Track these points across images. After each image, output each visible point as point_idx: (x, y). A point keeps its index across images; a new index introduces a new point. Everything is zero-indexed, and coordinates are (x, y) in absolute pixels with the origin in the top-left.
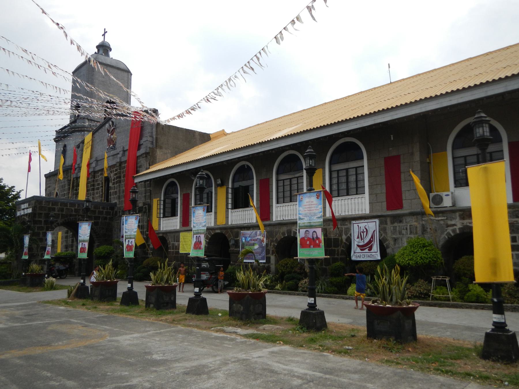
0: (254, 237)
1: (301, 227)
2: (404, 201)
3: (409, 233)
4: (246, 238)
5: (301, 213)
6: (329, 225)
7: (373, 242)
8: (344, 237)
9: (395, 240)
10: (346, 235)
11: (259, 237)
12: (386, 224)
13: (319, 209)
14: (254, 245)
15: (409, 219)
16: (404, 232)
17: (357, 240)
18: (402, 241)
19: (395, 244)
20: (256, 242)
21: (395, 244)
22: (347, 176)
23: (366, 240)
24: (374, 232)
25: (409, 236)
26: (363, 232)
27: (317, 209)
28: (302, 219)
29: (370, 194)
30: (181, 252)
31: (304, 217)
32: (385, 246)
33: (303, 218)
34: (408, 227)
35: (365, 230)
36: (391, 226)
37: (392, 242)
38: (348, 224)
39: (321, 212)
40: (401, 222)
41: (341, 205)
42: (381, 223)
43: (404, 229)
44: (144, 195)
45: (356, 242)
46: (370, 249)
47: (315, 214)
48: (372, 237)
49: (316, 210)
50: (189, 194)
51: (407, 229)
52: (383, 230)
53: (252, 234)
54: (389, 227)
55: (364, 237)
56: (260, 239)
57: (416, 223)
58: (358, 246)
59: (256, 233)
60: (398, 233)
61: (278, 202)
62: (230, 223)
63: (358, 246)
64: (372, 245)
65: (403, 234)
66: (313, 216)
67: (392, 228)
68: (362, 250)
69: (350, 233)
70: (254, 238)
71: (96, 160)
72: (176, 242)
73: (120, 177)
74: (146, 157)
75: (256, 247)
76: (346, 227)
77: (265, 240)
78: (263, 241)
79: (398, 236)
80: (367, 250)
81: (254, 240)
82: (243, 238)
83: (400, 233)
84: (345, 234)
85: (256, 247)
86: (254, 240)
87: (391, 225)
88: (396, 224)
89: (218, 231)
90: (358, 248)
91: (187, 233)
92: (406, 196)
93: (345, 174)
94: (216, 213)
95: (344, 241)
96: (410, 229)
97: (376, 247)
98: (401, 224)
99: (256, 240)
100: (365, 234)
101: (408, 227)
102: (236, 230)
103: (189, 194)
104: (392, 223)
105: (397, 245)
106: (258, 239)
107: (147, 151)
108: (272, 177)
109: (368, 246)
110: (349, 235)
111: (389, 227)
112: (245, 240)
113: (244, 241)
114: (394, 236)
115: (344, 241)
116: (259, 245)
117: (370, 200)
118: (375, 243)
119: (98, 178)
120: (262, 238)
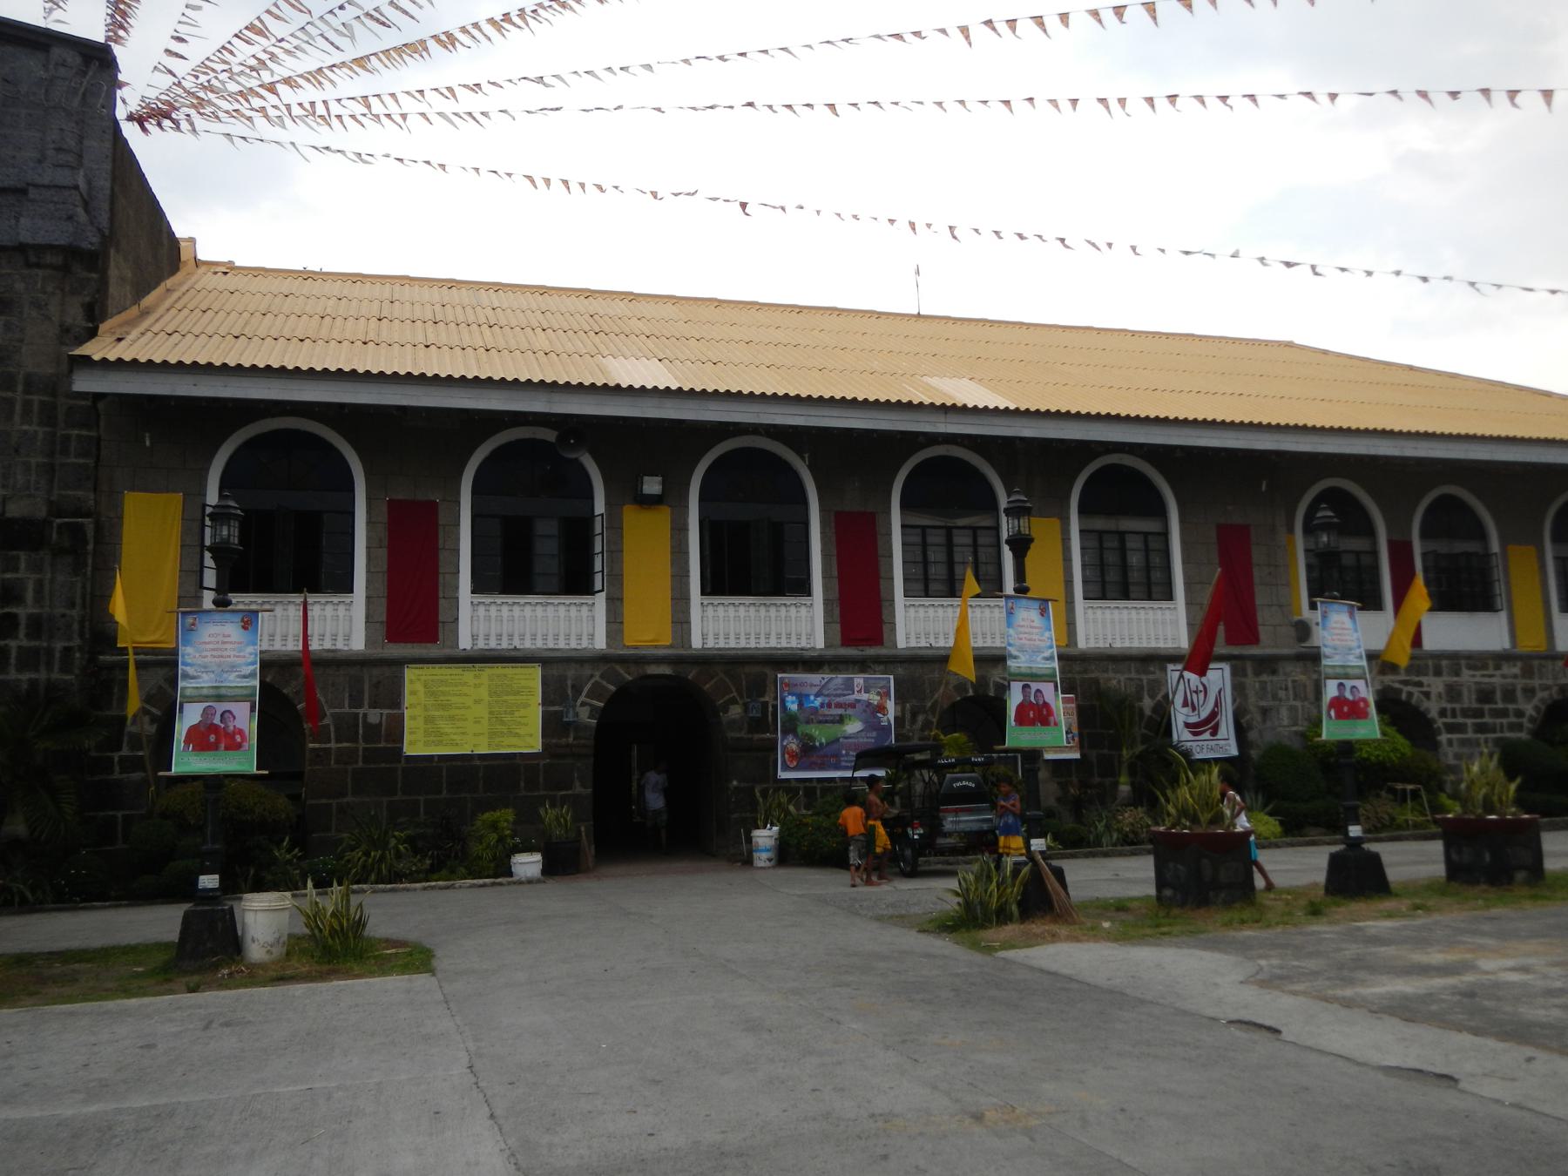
0: (839, 696)
1: (1020, 676)
2: (1261, 629)
3: (1291, 697)
4: (801, 698)
5: (189, 661)
6: (1104, 671)
7: (1219, 717)
8: (1147, 704)
9: (1265, 712)
10: (1152, 697)
11: (864, 697)
12: (1245, 675)
13: (247, 655)
14: (841, 720)
15: (1289, 667)
16: (1282, 694)
17: (1186, 710)
18: (1278, 713)
19: (1264, 721)
20: (850, 711)
21: (1264, 721)
22: (1123, 551)
23: (1205, 714)
24: (1220, 692)
25: (1293, 703)
26: (1196, 692)
27: (242, 654)
28: (193, 678)
29: (1189, 603)
30: (410, 749)
31: (199, 674)
32: (1245, 725)
33: (195, 674)
34: (1290, 685)
35: (1201, 688)
36: (1255, 682)
37: (1258, 718)
38: (1158, 672)
39: (253, 663)
40: (1274, 672)
41: (1113, 621)
42: (1234, 674)
43: (1281, 689)
44: (41, 459)
45: (1180, 716)
46: (1215, 731)
47: (233, 667)
48: (1216, 705)
49: (238, 657)
50: (432, 508)
51: (1286, 689)
52: (1238, 689)
53: (832, 685)
54: (1251, 681)
55: (1201, 702)
56: (869, 704)
57: (1303, 677)
58: (1187, 725)
59: (849, 686)
60: (1270, 696)
62: (696, 643)
63: (1187, 725)
64: (1218, 721)
65: (1280, 700)
66: (227, 672)
67: (1257, 685)
68: (1195, 734)
69: (1162, 693)
70: (841, 700)
72: (374, 705)
74: (65, 269)
75: (853, 727)
76: (1151, 677)
77: (891, 706)
78: (881, 708)
79: (1271, 703)
80: (1207, 736)
81: (839, 706)
83: (1275, 697)
84: (1149, 695)
85: (853, 727)
86: (839, 706)
87: (1256, 680)
88: (1265, 677)
89: (665, 670)
90: (1186, 730)
91: (459, 671)
92: (1266, 618)
93: (1115, 544)
94: (615, 604)
95: (1148, 712)
96: (1294, 688)
97: (1227, 728)
98: (1275, 678)
99: (852, 705)
100: (1201, 696)
101: (1290, 685)
102: (756, 669)
104: (1257, 673)
105: (1269, 724)
106: (858, 701)
107: (85, 245)
109: (1209, 724)
110: (1159, 697)
111: (1251, 681)
112: (800, 705)
114: (1263, 703)
115: (1148, 712)
116: (865, 722)
117: (1188, 618)
118: (1224, 718)
120: (875, 699)
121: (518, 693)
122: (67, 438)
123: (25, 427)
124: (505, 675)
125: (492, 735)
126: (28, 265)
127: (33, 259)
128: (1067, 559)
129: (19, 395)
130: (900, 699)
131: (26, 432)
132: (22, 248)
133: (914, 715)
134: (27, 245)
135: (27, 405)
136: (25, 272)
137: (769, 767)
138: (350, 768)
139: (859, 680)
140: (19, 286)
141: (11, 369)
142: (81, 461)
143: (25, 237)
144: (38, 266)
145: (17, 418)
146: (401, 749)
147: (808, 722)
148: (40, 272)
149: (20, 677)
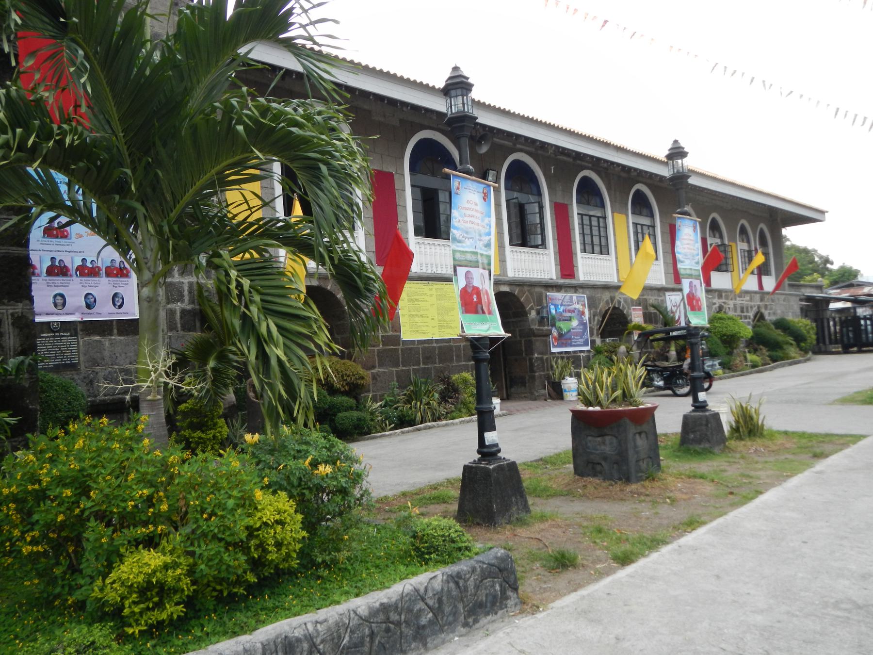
0: (569, 305)
4: (556, 306)
20: (573, 315)
30: (405, 337)
53: (565, 300)
56: (579, 311)
61: (584, 250)
70: (569, 308)
75: (575, 323)
78: (583, 313)
81: (569, 311)
82: (552, 307)
85: (575, 323)
86: (569, 311)
91: (422, 286)
99: (573, 311)
102: (538, 290)
103: (391, 175)
106: (575, 309)
108: (572, 204)
112: (556, 310)
113: (553, 311)
116: (579, 321)
121: (449, 301)
124: (443, 289)
125: (441, 327)
128: (629, 237)
130: (590, 308)
133: (594, 316)
137: (547, 346)
138: (376, 349)
139: (575, 296)
146: (400, 336)
147: (560, 320)
149: (182, 280)
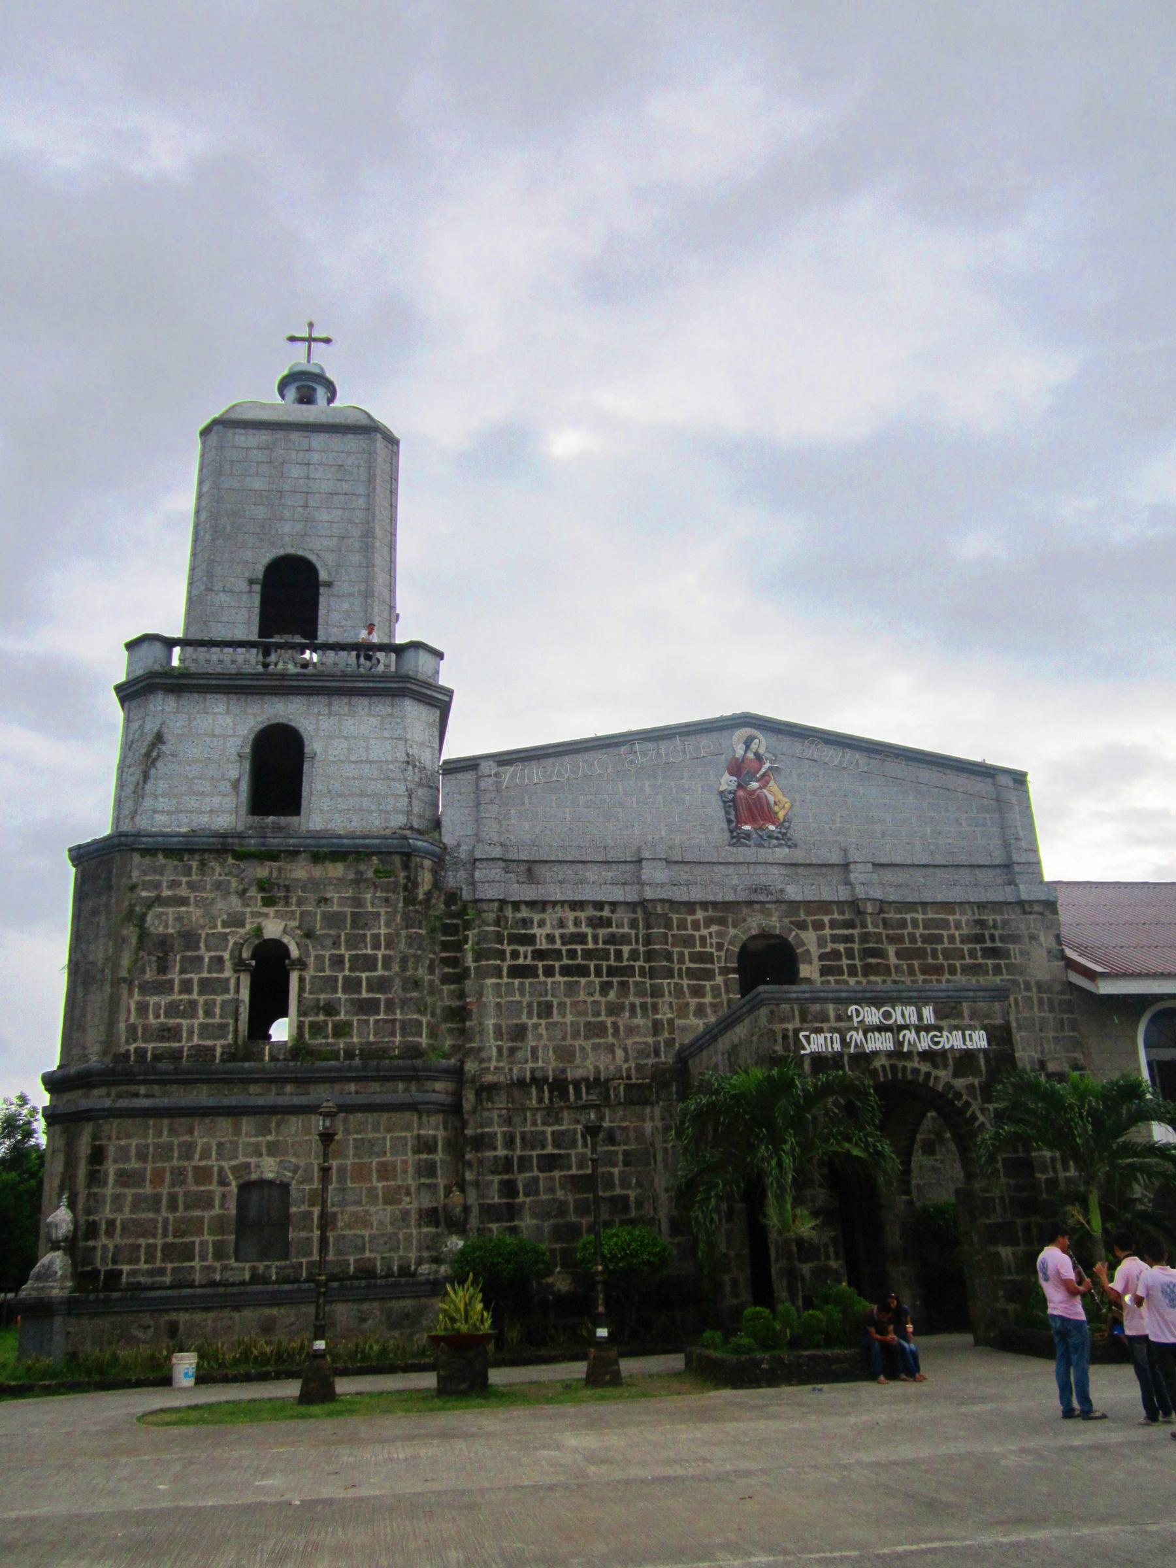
71: (665, 859)
73: (880, 953)
119: (690, 932)
122: (1062, 1021)
123: (1043, 1014)
126: (1025, 913)
127: (1028, 909)
129: (1034, 993)
131: (1043, 1018)
132: (1021, 903)
134: (1026, 901)
135: (1041, 1000)
136: (1022, 917)
140: (1023, 926)
141: (1028, 978)
142: (1071, 1034)
143: (1024, 896)
144: (1030, 913)
145: (1036, 1009)
148: (1032, 917)
